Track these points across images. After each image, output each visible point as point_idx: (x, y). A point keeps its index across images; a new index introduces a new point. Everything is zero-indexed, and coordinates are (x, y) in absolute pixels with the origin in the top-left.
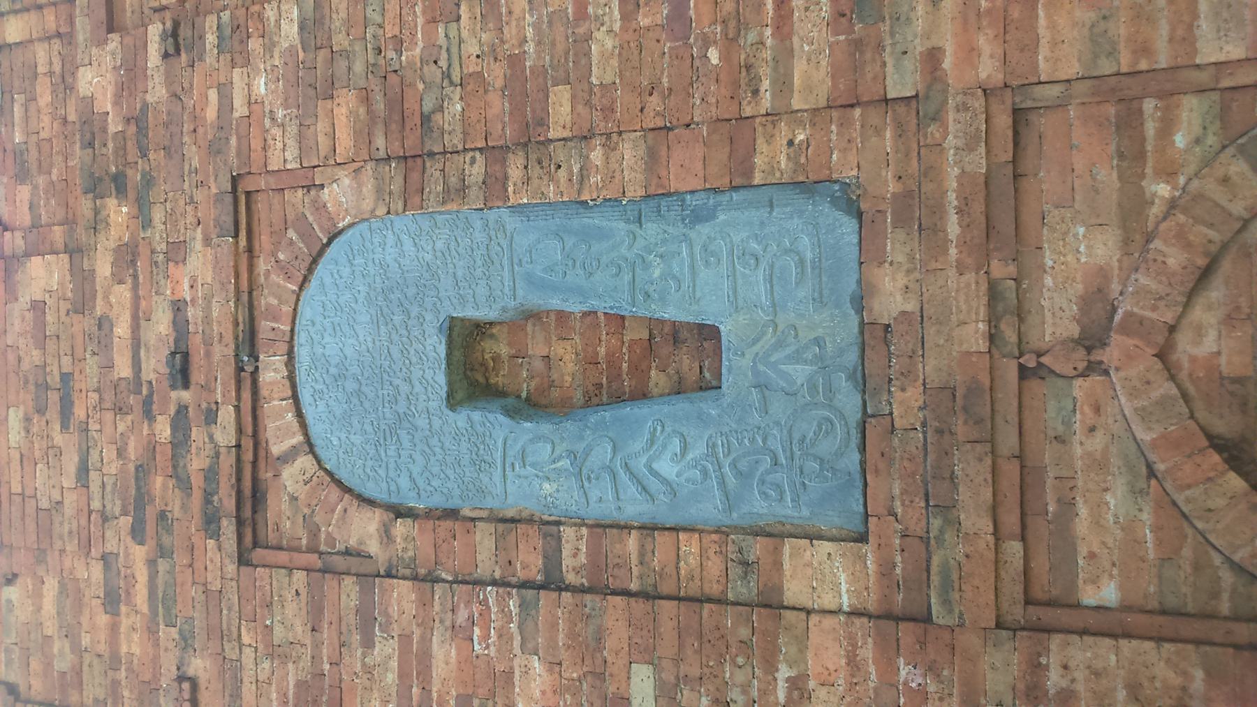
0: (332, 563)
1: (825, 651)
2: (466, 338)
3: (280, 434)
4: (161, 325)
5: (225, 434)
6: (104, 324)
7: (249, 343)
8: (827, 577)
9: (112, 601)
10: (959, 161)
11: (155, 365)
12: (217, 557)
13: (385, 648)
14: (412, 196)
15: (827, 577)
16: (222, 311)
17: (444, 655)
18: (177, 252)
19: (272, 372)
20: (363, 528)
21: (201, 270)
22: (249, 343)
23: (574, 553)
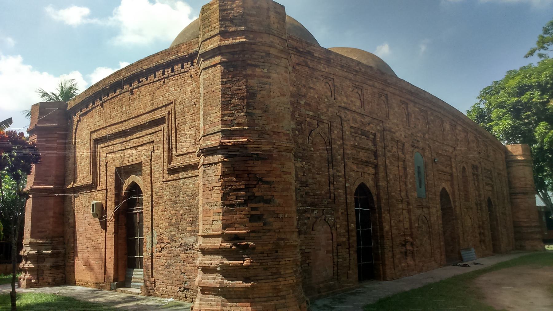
4: (419, 140)
5: (416, 145)
7: (418, 148)
9: (408, 129)
22: (418, 148)
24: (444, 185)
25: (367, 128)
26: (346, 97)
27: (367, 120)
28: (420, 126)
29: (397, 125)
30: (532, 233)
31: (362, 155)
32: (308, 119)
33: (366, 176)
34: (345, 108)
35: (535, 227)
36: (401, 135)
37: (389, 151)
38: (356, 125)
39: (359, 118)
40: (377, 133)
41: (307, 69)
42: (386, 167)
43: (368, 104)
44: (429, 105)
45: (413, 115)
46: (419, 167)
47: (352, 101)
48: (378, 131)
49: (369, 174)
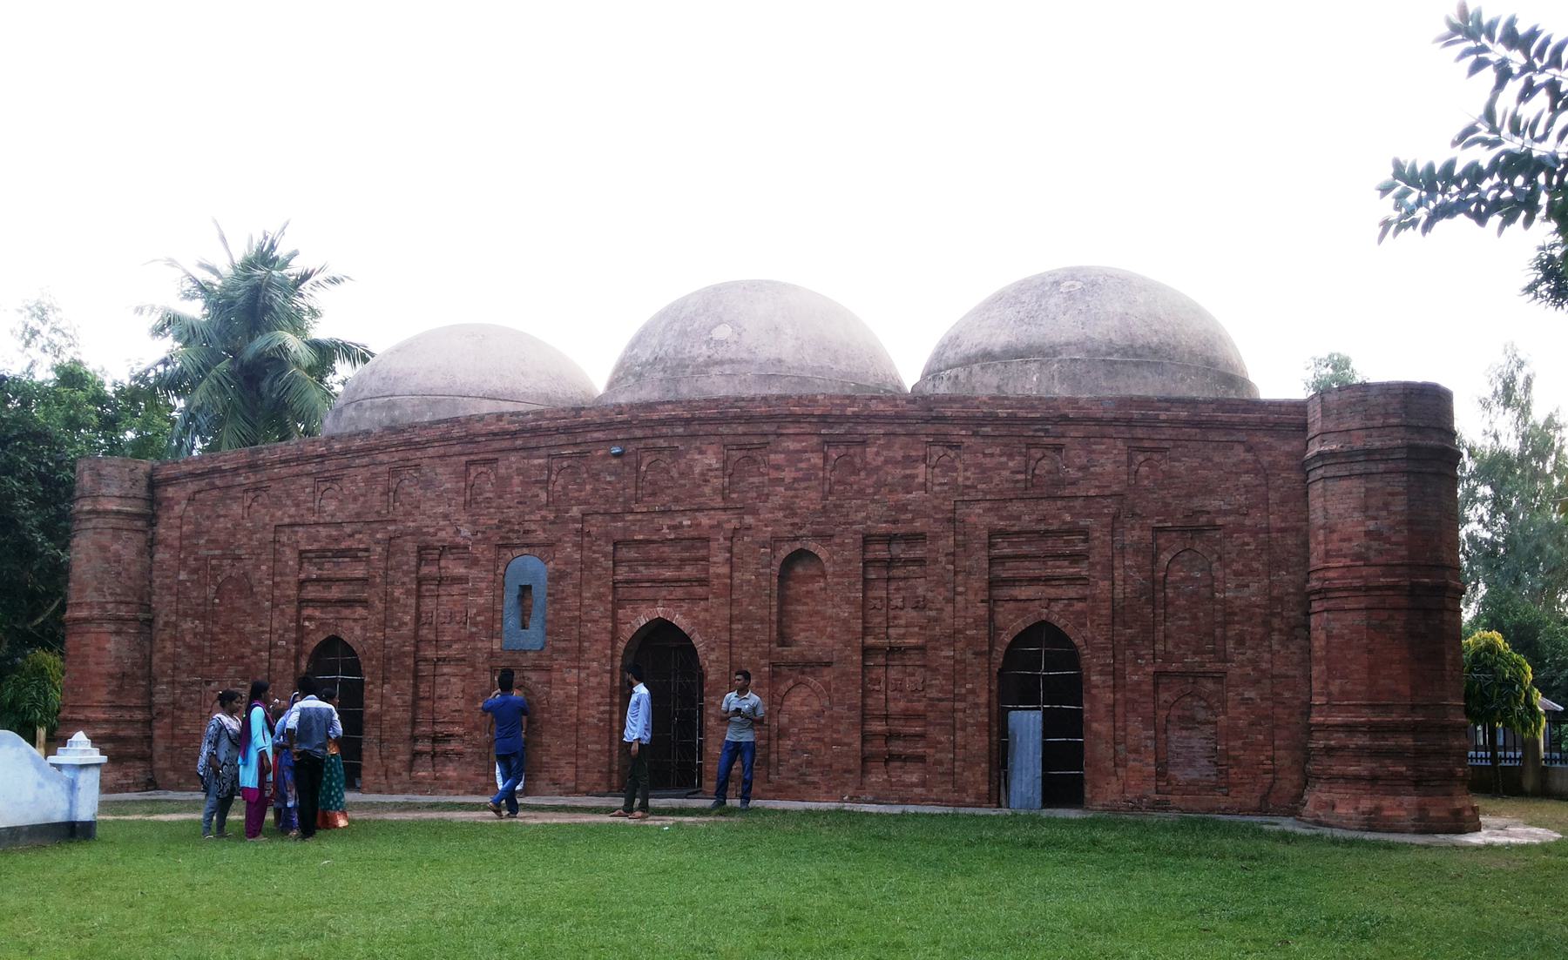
0: (495, 562)
1: (488, 645)
2: (530, 587)
3: (516, 552)
4: (533, 527)
5: (516, 541)
6: (532, 512)
8: (496, 645)
10: (545, 663)
11: (527, 526)
12: (496, 539)
13: (484, 574)
14: (550, 579)
15: (496, 645)
16: (535, 541)
17: (484, 585)
18: (544, 531)
19: (525, 550)
20: (501, 570)
21: (541, 536)
23: (499, 607)
24: (660, 612)
25: (343, 546)
26: (297, 505)
27: (348, 530)
28: (543, 496)
29: (446, 516)
30: (1329, 751)
31: (335, 593)
32: (214, 562)
33: (345, 624)
34: (291, 525)
35: (1350, 728)
36: (458, 531)
37: (406, 573)
38: (315, 546)
39: (323, 531)
40: (373, 547)
41: (215, 492)
42: (389, 601)
43: (355, 499)
44: (596, 435)
45: (517, 480)
46: (525, 590)
47: (309, 509)
48: (378, 542)
49: (355, 620)
